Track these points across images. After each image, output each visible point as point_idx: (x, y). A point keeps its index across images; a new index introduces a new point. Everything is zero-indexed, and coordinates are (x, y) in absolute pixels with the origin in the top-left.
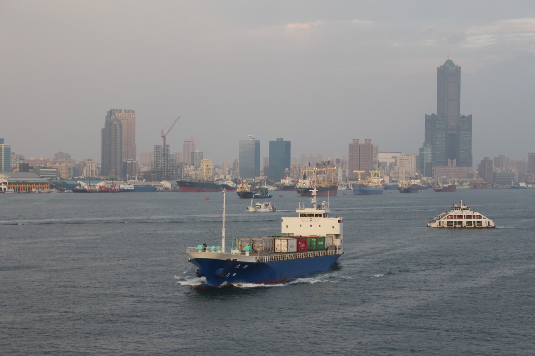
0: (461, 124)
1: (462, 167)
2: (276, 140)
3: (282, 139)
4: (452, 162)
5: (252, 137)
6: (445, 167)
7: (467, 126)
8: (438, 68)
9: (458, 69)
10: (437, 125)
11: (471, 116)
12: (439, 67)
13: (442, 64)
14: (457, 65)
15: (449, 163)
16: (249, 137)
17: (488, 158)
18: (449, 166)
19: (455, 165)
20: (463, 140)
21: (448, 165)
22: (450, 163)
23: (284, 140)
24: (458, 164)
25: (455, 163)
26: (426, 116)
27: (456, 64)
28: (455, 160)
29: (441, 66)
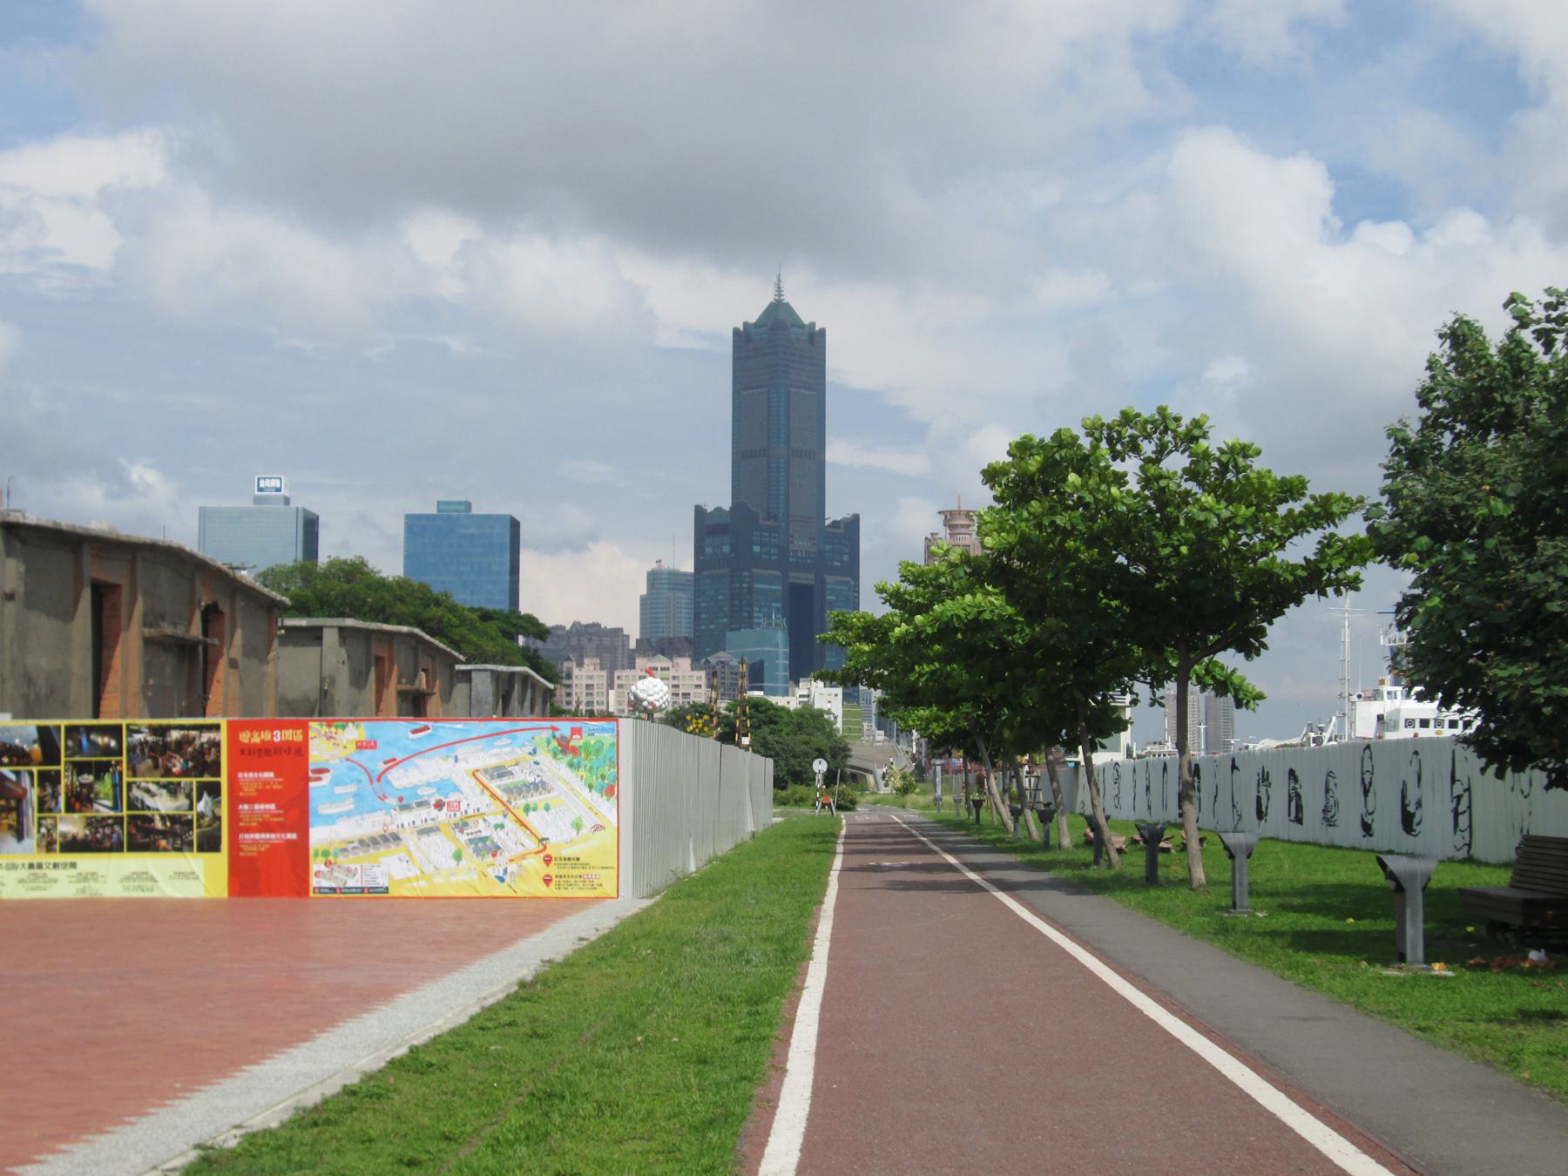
0: (827, 548)
2: (434, 512)
3: (468, 505)
5: (279, 490)
7: (846, 558)
8: (736, 331)
9: (816, 339)
10: (756, 549)
12: (742, 328)
13: (753, 319)
14: (813, 324)
16: (260, 490)
23: (475, 511)
26: (699, 511)
27: (806, 321)
29: (745, 324)
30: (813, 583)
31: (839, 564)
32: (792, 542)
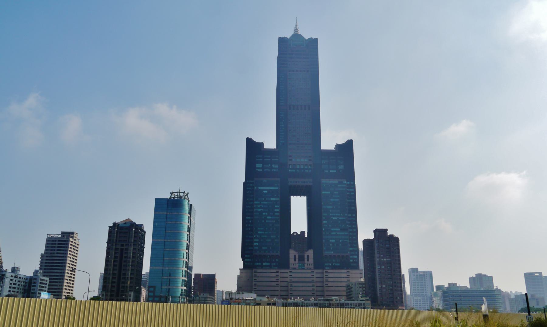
0: (324, 162)
1: (329, 271)
4: (301, 259)
6: (283, 271)
7: (341, 167)
10: (259, 166)
11: (350, 143)
15: (292, 260)
17: (385, 231)
18: (295, 269)
19: (312, 266)
20: (332, 200)
21: (291, 266)
22: (295, 260)
24: (319, 264)
25: (311, 261)
28: (310, 253)
30: (311, 184)
31: (335, 171)
32: (291, 160)
